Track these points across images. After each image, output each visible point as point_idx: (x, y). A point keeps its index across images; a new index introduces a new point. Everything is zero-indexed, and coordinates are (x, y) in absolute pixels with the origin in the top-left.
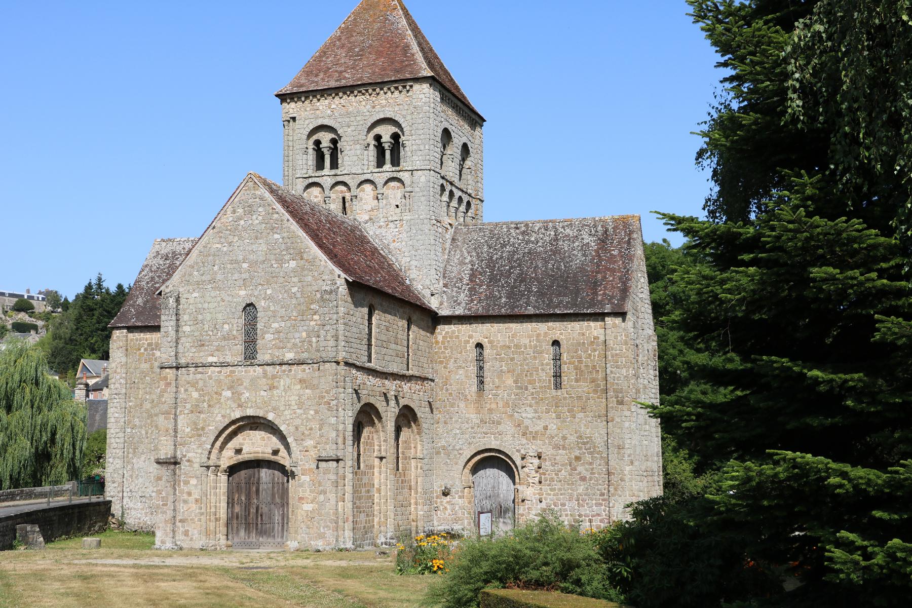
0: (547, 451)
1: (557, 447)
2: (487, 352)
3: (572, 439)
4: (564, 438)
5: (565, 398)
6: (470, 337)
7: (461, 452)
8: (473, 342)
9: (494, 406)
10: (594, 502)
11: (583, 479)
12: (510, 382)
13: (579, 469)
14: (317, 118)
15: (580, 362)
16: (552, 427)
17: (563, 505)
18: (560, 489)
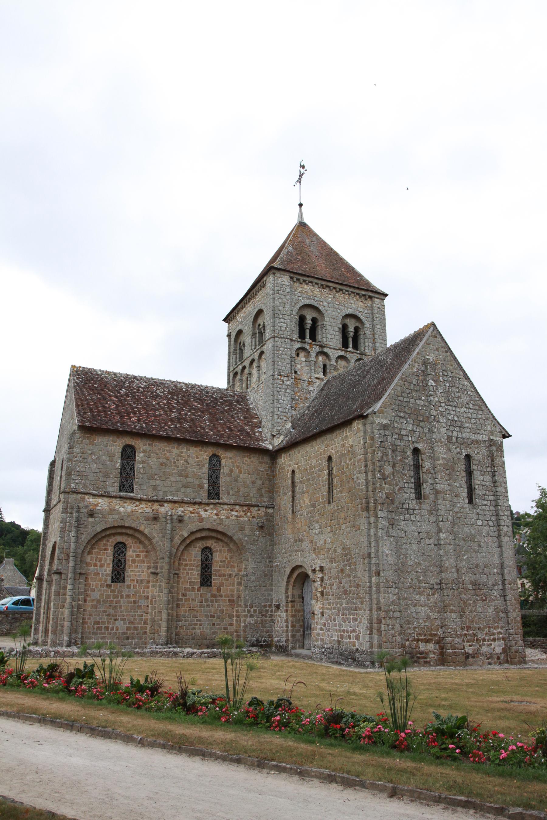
0: (326, 564)
1: (331, 562)
2: (297, 476)
3: (339, 550)
4: (335, 551)
5: (335, 511)
6: (290, 466)
7: (285, 569)
8: (291, 469)
9: (300, 526)
10: (352, 617)
11: (345, 592)
12: (307, 501)
13: (343, 581)
14: (237, 326)
15: (343, 473)
16: (329, 540)
17: (335, 620)
18: (333, 604)
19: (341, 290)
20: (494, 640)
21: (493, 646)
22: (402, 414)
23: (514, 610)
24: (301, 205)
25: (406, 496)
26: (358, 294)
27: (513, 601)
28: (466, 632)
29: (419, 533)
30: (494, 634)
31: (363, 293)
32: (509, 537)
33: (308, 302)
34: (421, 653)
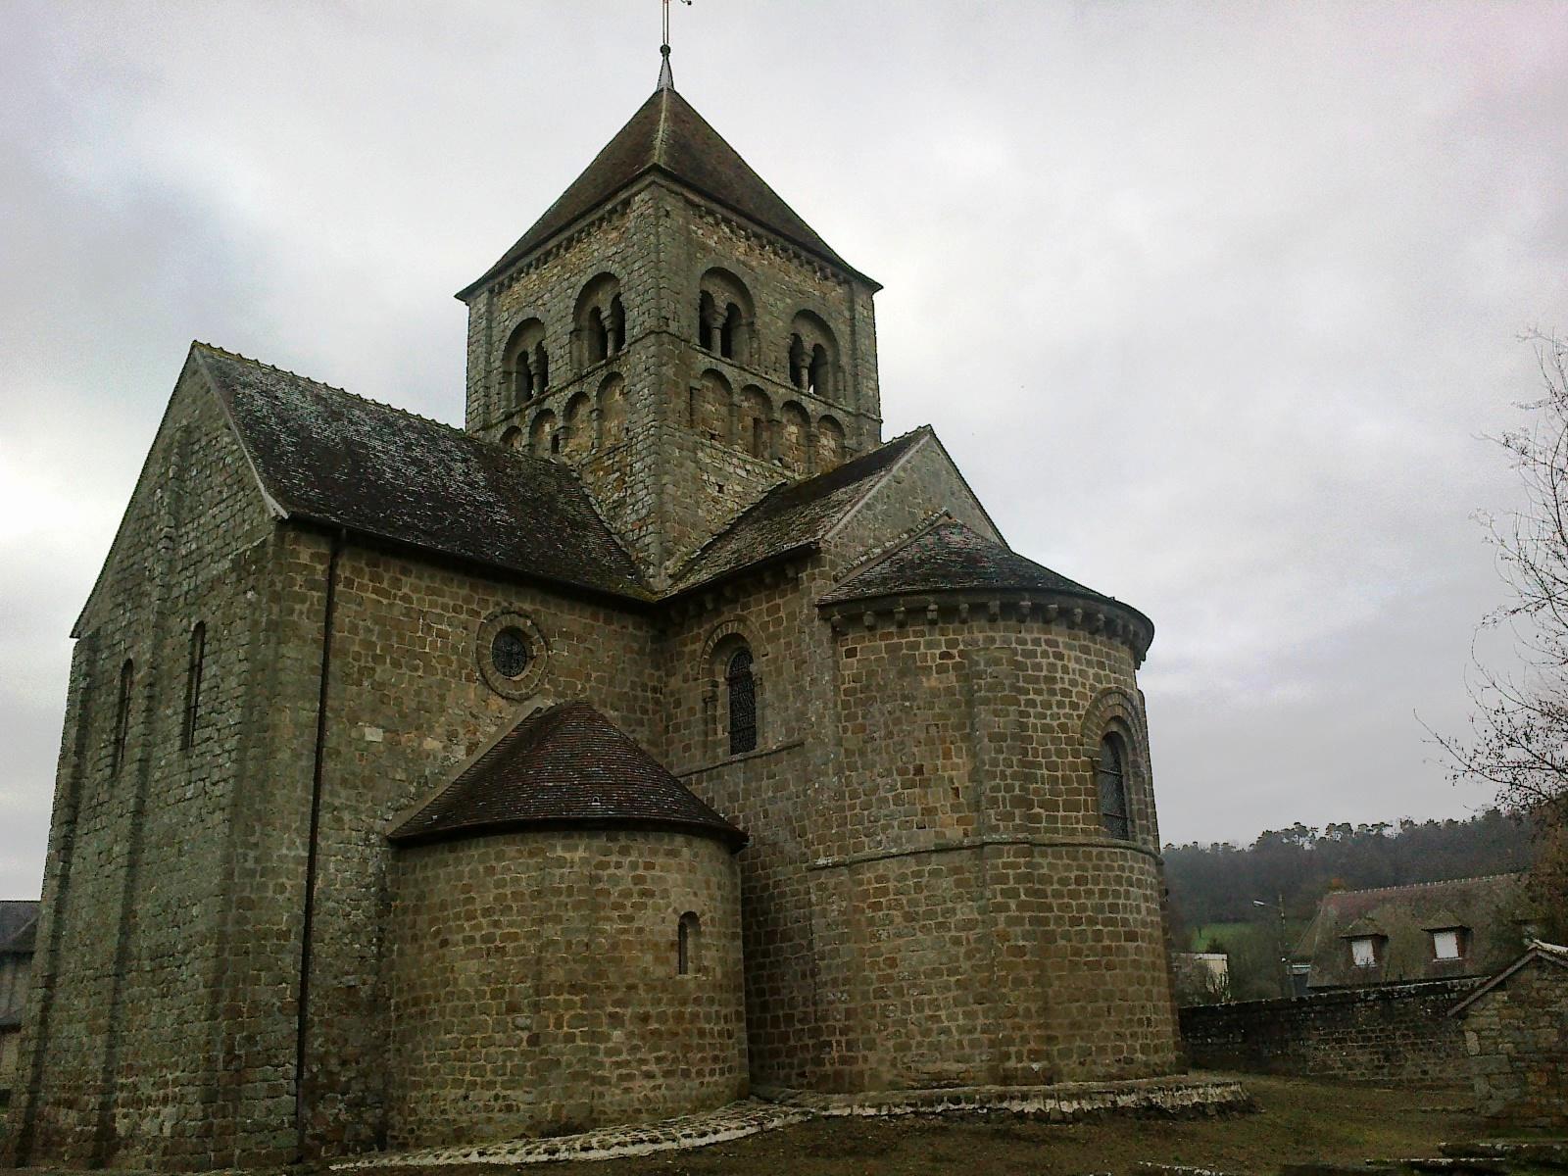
19: (570, 240)
20: (165, 1101)
21: (162, 1117)
22: (120, 600)
23: (197, 1018)
24: (665, 50)
25: (98, 776)
26: (601, 219)
27: (202, 990)
28: (124, 1081)
29: (100, 853)
30: (166, 1084)
31: (609, 207)
32: (223, 809)
33: (519, 319)
34: (57, 1131)
